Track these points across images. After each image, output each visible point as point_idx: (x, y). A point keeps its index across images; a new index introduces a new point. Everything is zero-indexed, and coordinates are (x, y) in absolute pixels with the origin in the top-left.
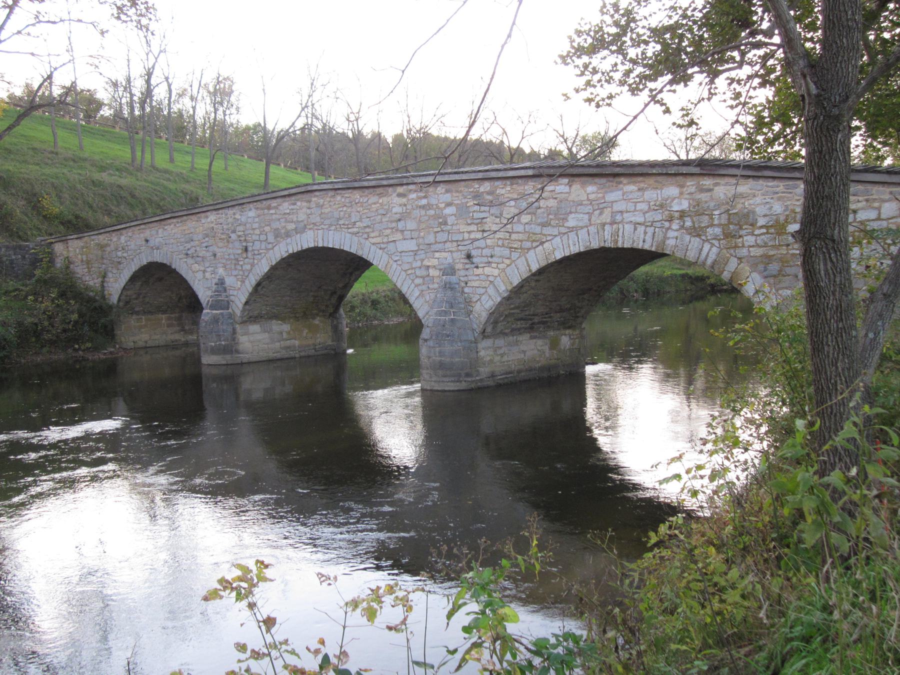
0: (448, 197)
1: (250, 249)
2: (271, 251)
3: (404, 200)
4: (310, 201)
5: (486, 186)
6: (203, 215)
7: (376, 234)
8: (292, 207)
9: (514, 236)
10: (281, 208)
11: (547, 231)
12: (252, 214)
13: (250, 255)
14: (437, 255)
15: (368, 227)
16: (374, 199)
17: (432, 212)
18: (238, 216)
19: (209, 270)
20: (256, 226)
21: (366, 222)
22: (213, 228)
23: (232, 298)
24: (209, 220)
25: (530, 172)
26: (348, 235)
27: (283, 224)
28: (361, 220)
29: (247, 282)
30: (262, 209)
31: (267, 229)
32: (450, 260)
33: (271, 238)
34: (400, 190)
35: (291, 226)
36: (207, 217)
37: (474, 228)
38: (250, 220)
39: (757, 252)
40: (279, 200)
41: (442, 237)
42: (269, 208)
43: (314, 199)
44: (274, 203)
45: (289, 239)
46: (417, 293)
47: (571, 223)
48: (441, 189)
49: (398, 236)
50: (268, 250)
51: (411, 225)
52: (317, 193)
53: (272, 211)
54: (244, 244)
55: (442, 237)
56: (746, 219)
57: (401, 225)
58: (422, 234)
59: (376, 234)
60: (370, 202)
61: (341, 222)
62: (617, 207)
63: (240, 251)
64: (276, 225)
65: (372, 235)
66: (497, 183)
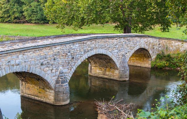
0: (123, 40)
1: (75, 57)
2: (82, 57)
3: (117, 41)
4: (96, 41)
5: (129, 38)
6: (53, 47)
7: (111, 49)
8: (91, 43)
9: (132, 47)
10: (87, 43)
11: (135, 46)
12: (77, 45)
13: (74, 59)
14: (121, 52)
15: (109, 47)
16: (111, 40)
17: (121, 43)
18: (72, 47)
19: (54, 69)
20: (78, 49)
21: (109, 46)
22: (59, 52)
23: (66, 77)
24: (57, 48)
25: (135, 36)
26: (104, 50)
27: (87, 48)
28: (108, 46)
29: (72, 69)
30: (81, 44)
31: (82, 50)
32: (123, 53)
33: (83, 53)
34: (116, 38)
35: (90, 48)
36: (56, 47)
37: (127, 46)
38: (76, 48)
39: (151, 47)
40: (87, 41)
41: (122, 48)
42: (83, 43)
43: (97, 40)
44: (85, 42)
45: (88, 53)
46: (117, 61)
47: (137, 45)
48: (122, 38)
49: (115, 49)
50: (81, 57)
51: (117, 46)
52: (98, 39)
53: (84, 44)
54: (73, 56)
55: (122, 48)
56: (150, 43)
57: (115, 47)
58: (119, 48)
59: (111, 49)
60: (110, 41)
61: (103, 46)
62: (141, 42)
63: (71, 59)
64: (85, 49)
65: (110, 49)
66: (130, 38)
